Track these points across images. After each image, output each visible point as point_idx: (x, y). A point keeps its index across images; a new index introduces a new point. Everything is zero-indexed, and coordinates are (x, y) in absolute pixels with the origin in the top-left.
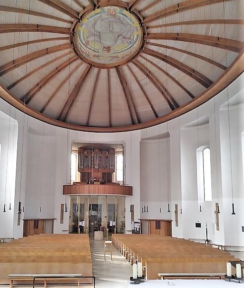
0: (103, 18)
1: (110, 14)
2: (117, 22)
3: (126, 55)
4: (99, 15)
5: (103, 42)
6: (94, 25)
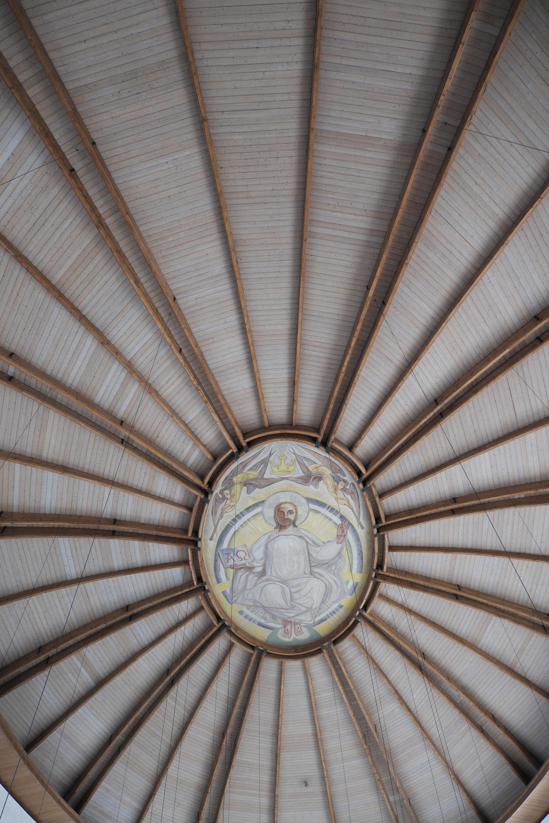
0: (309, 614)
1: (295, 624)
2: (276, 608)
3: (224, 498)
4: (317, 619)
5: (298, 544)
6: (327, 593)
